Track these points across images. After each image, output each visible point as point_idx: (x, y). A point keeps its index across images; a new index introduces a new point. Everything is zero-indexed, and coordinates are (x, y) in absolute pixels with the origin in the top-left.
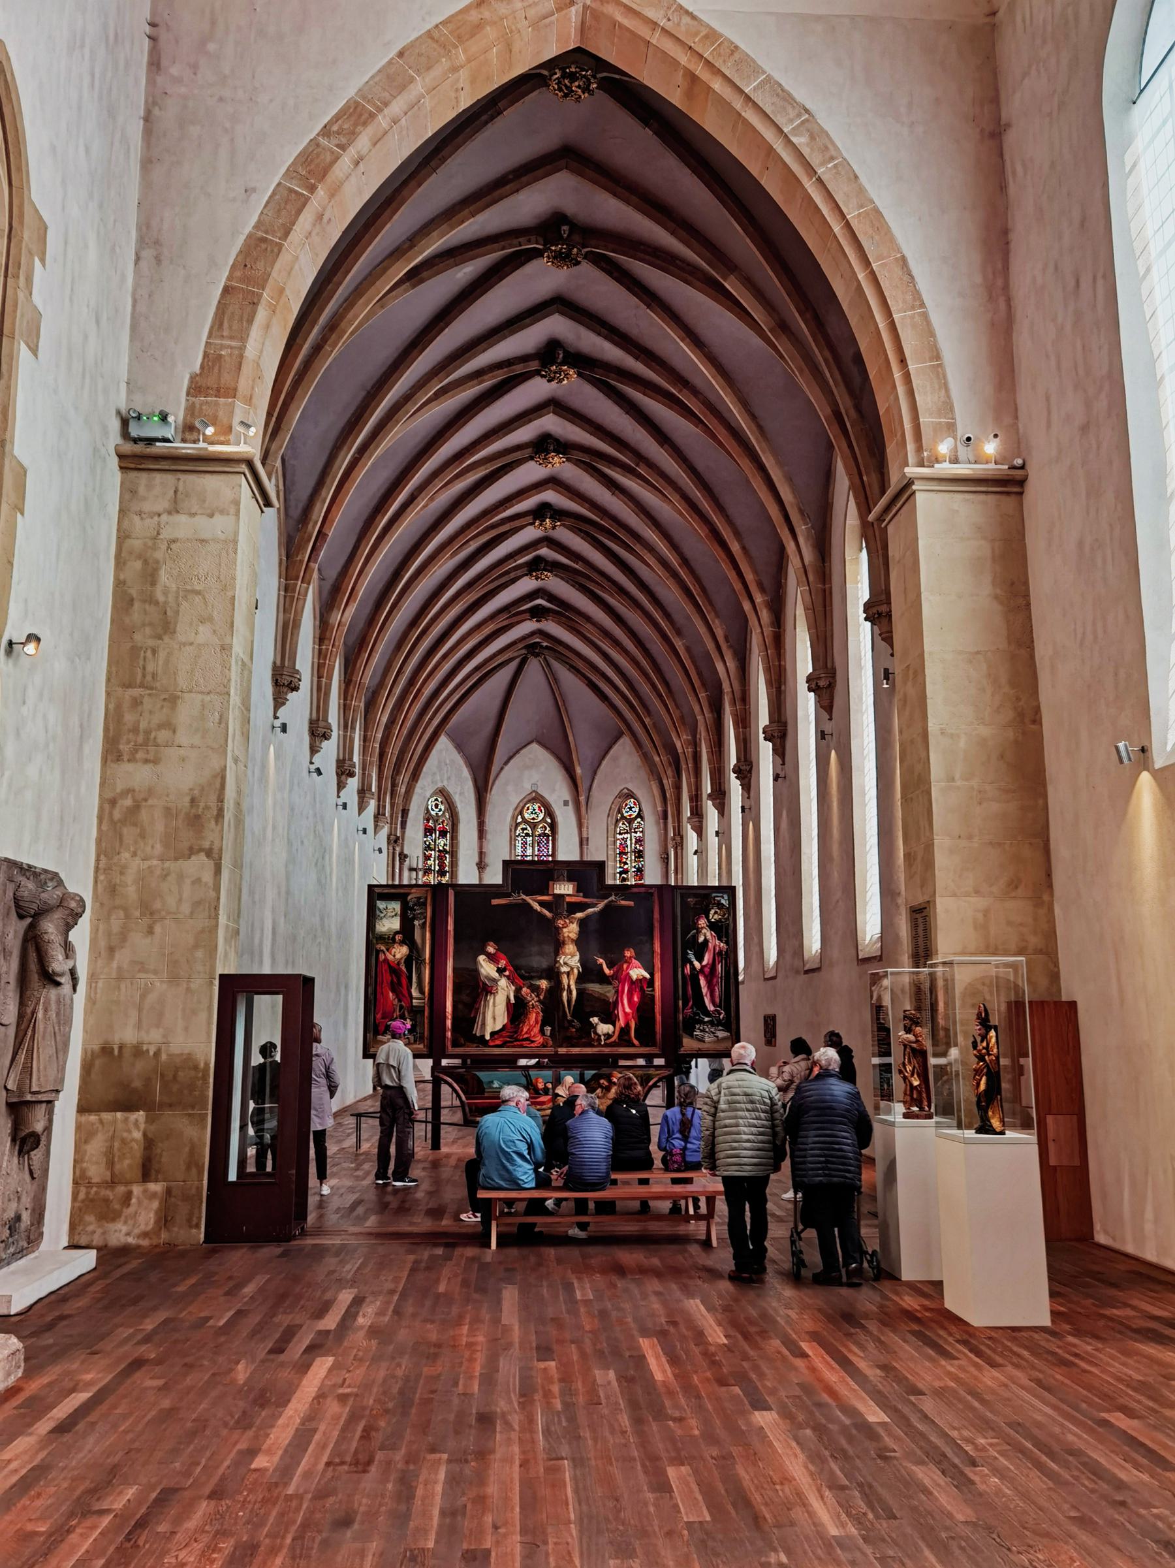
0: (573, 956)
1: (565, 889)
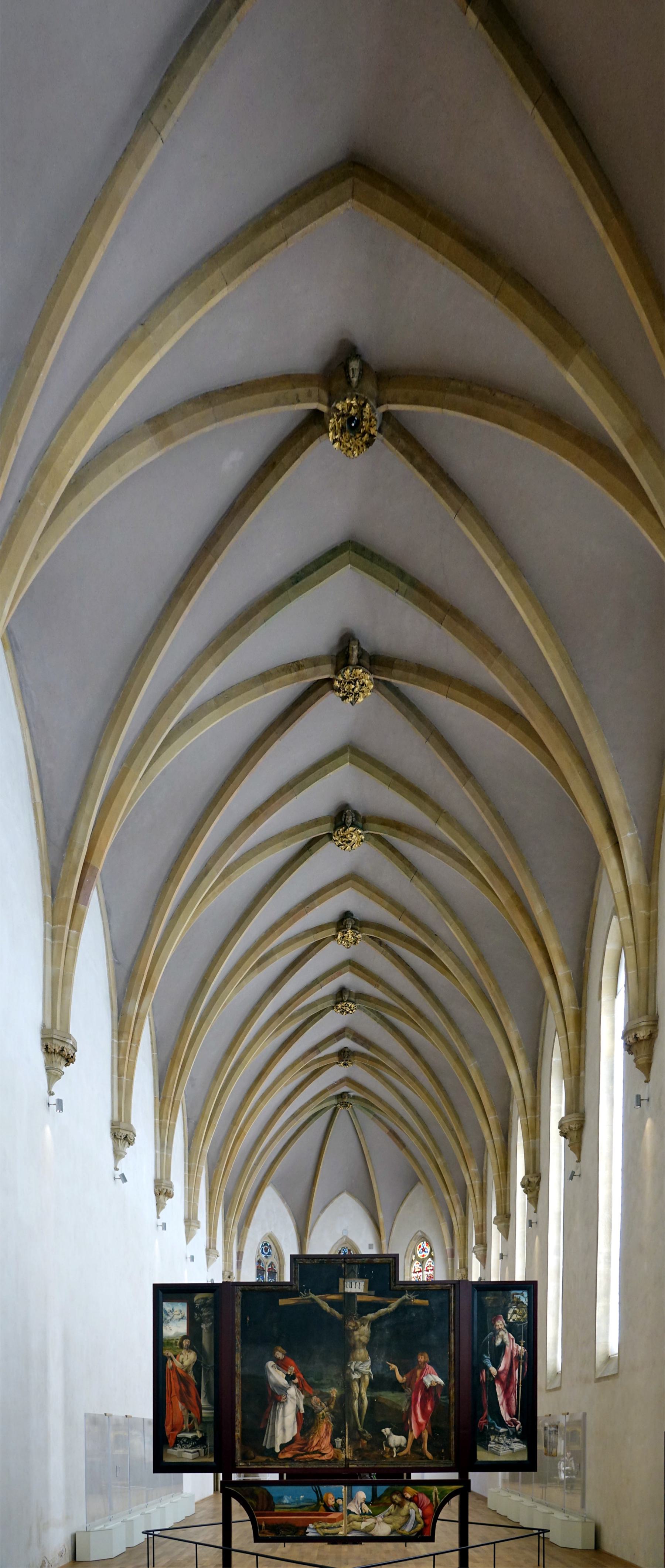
0: (364, 1361)
1: (356, 1287)
